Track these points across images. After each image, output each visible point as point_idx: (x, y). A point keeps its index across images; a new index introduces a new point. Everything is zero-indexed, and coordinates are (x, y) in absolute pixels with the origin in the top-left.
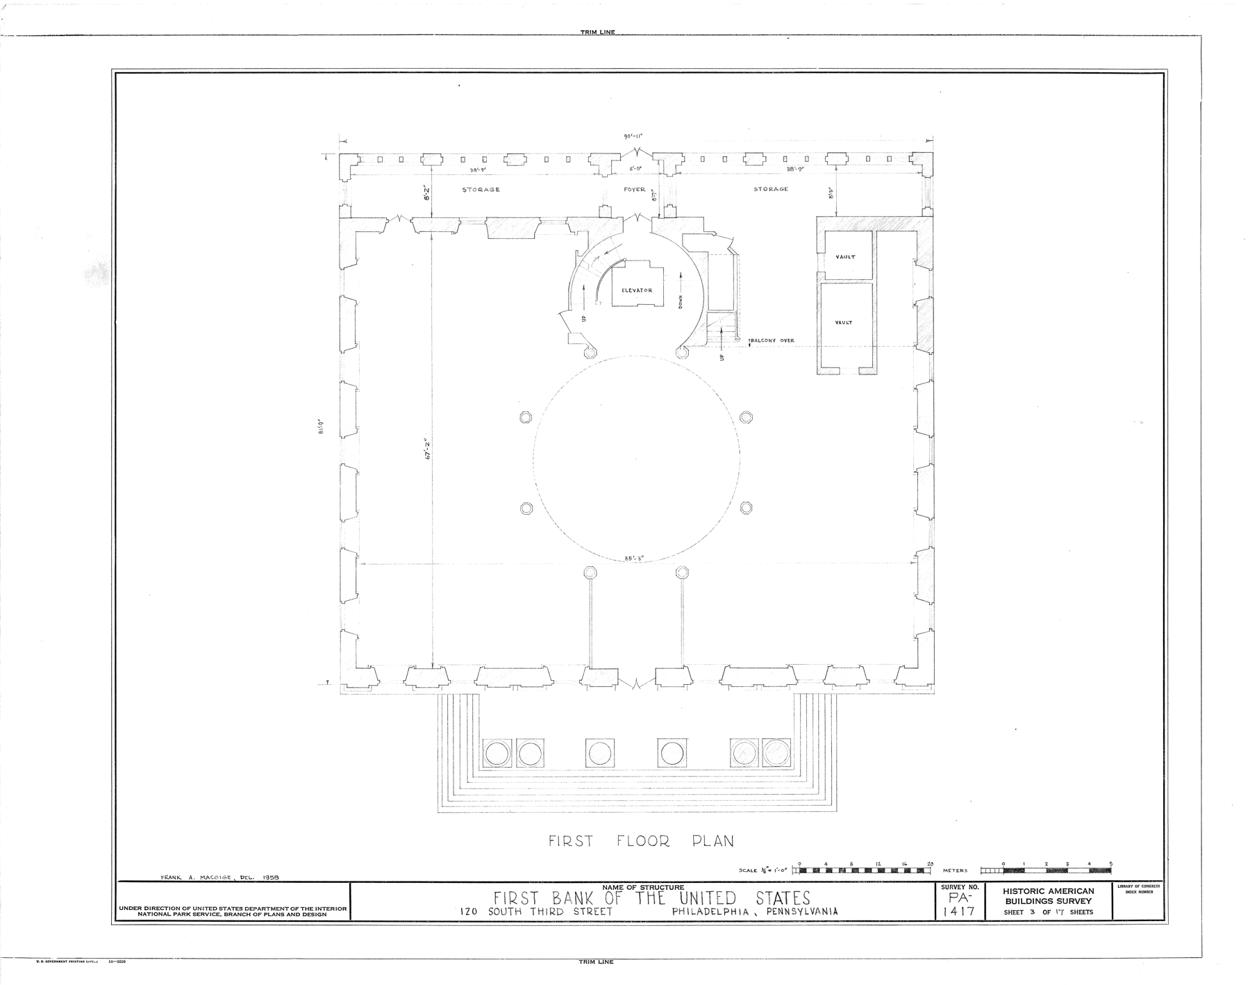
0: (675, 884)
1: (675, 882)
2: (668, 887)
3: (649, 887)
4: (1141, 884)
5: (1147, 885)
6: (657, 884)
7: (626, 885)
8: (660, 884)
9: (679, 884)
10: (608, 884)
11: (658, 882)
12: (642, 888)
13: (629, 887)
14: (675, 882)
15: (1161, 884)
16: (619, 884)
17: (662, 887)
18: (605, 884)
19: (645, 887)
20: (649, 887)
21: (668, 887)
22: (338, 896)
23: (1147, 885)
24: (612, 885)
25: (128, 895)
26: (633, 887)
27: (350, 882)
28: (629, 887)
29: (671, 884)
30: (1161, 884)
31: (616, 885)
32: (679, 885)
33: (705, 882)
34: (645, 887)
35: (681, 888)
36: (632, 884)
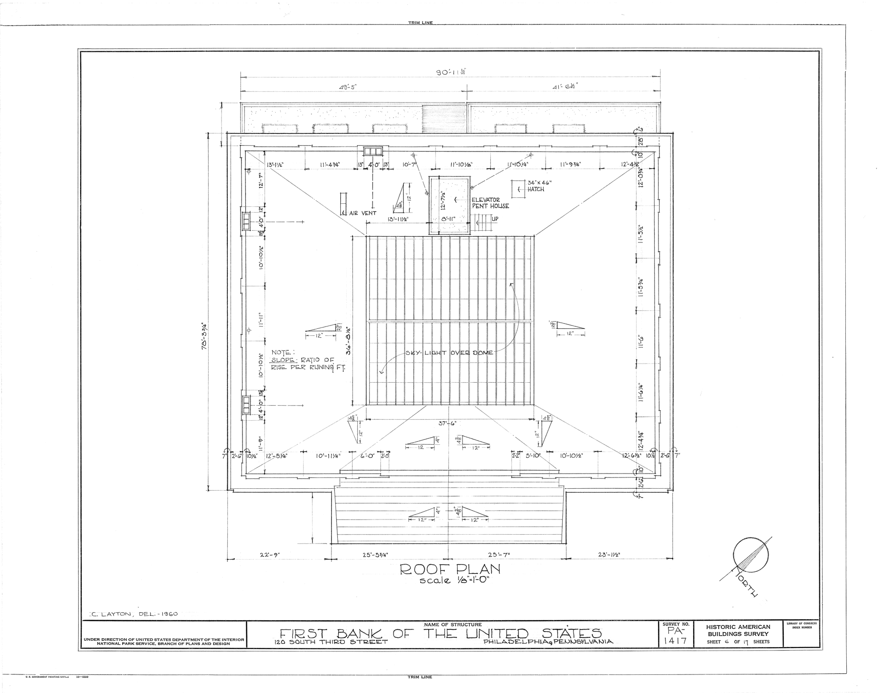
0: (475, 622)
1: (475, 621)
2: (471, 624)
3: (457, 625)
4: (803, 622)
5: (808, 623)
6: (463, 622)
7: (440, 623)
8: (465, 622)
9: (478, 622)
10: (428, 622)
11: (463, 621)
12: (452, 625)
13: (443, 625)
14: (475, 621)
15: (818, 622)
16: (436, 622)
17: (466, 625)
18: (426, 622)
19: (454, 624)
20: (457, 625)
21: (471, 624)
22: (238, 630)
23: (808, 623)
24: (431, 623)
25: (90, 630)
26: (446, 624)
27: (246, 621)
28: (443, 625)
29: (473, 622)
30: (818, 622)
31: (434, 623)
32: (478, 622)
33: (490, 621)
34: (454, 624)
35: (480, 625)
36: (445, 622)
